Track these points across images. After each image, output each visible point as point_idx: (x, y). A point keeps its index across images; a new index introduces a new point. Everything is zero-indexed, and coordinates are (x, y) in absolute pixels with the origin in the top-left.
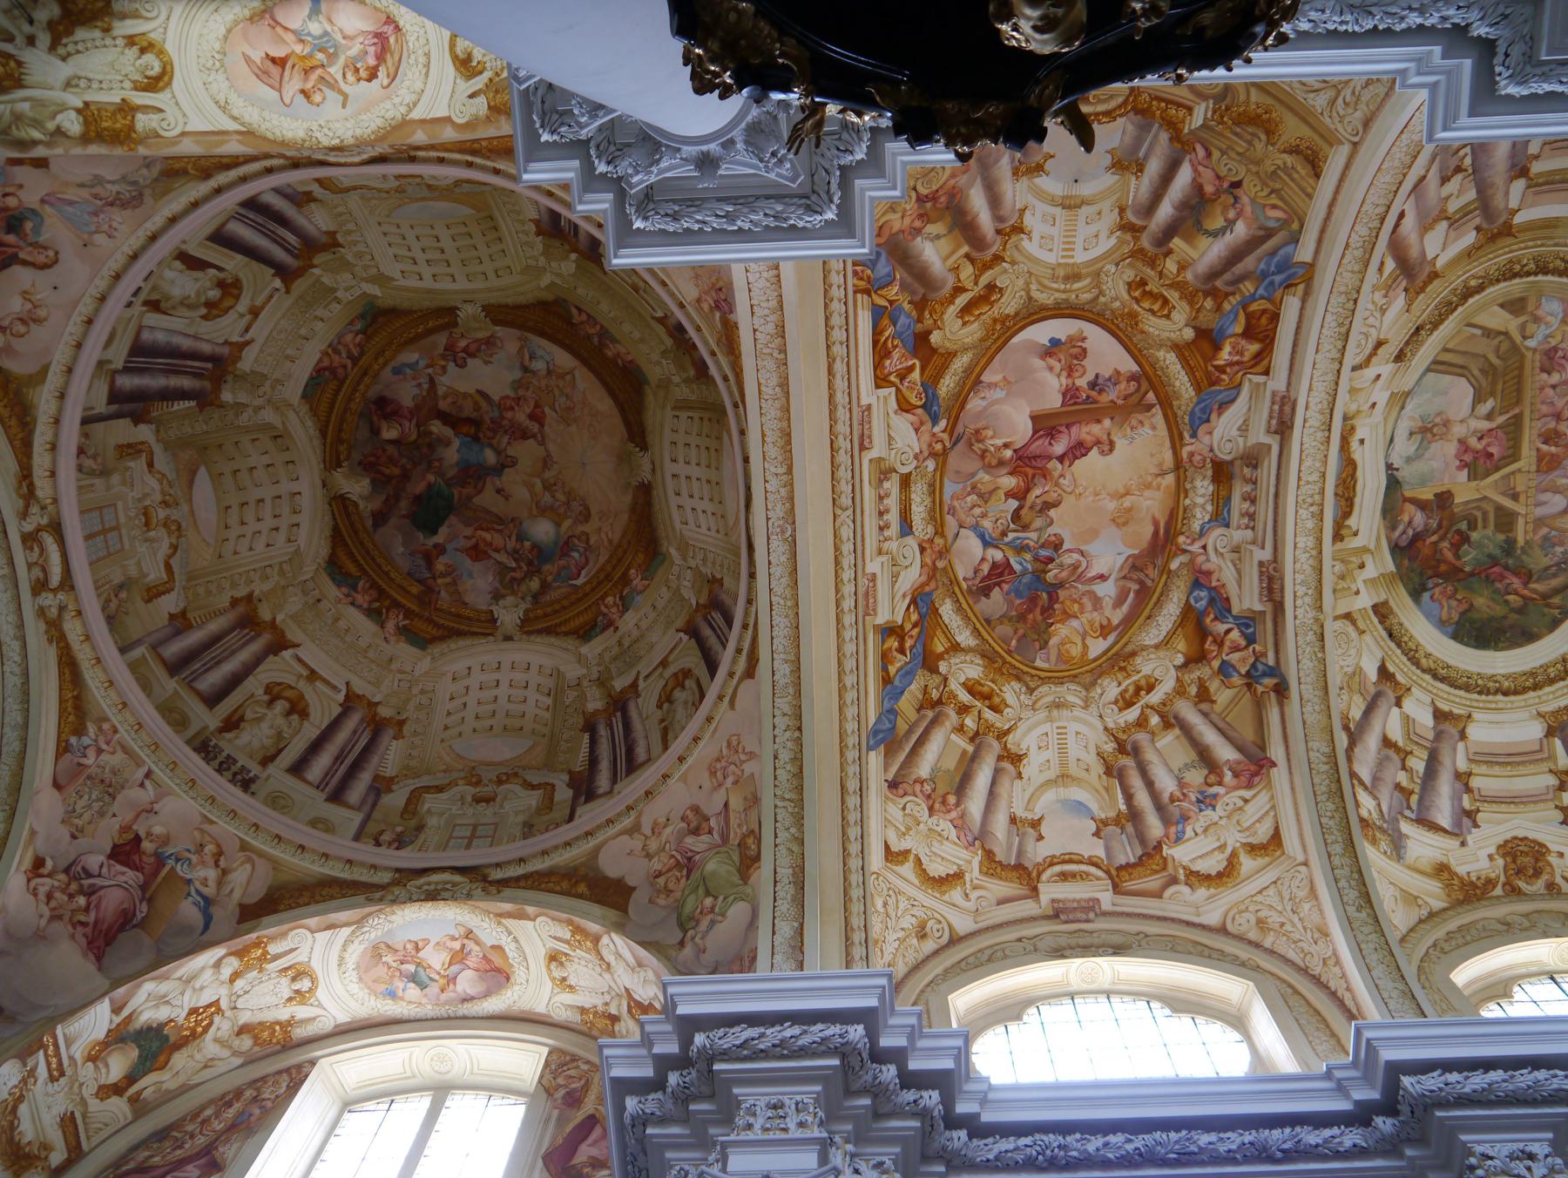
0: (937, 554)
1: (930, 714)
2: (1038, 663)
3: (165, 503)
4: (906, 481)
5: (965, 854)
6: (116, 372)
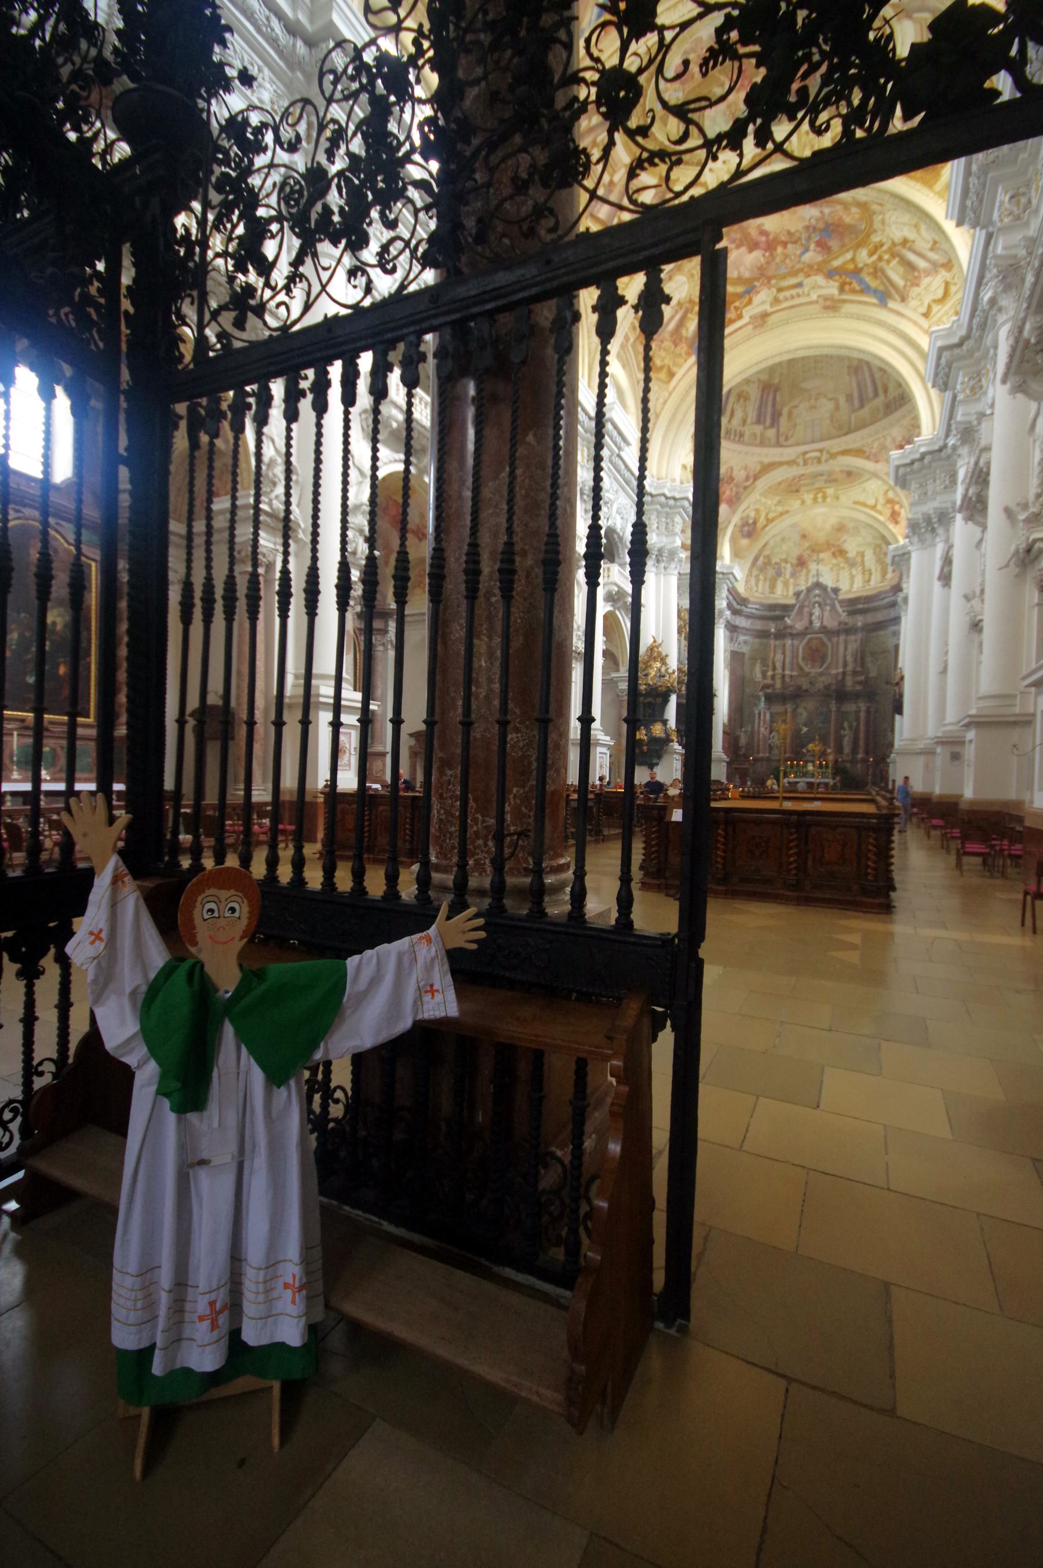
0: (811, 270)
1: (879, 274)
2: (863, 227)
3: (809, 400)
4: (780, 290)
5: (940, 276)
6: (765, 428)
